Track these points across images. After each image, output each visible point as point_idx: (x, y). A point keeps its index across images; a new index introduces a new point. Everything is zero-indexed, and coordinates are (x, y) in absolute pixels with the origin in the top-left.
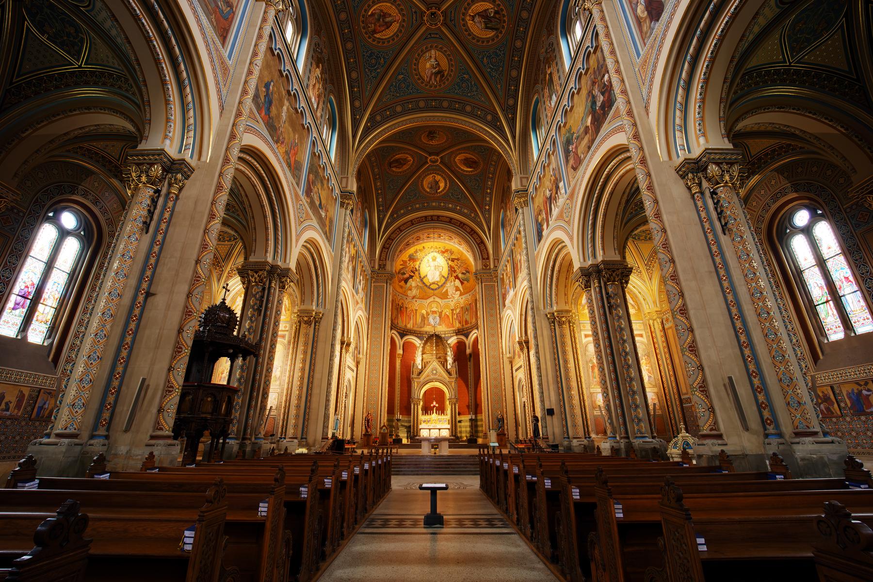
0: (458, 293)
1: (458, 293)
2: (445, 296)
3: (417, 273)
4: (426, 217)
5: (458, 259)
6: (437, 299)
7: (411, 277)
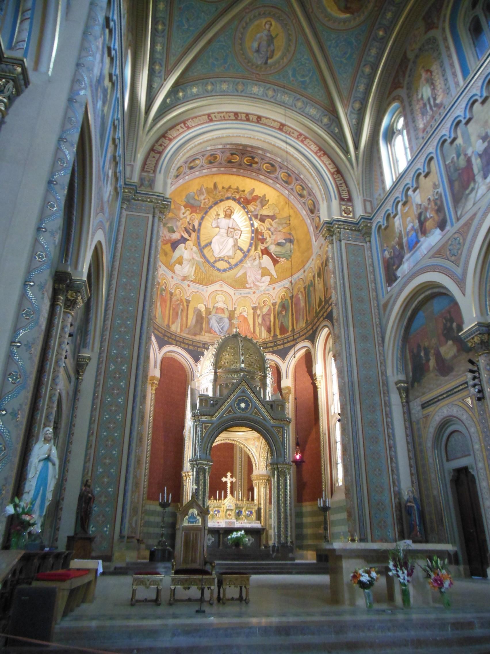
0: (267, 279)
1: (267, 279)
2: (241, 283)
3: (194, 235)
4: (236, 114)
5: (273, 218)
6: (226, 288)
7: (184, 240)
